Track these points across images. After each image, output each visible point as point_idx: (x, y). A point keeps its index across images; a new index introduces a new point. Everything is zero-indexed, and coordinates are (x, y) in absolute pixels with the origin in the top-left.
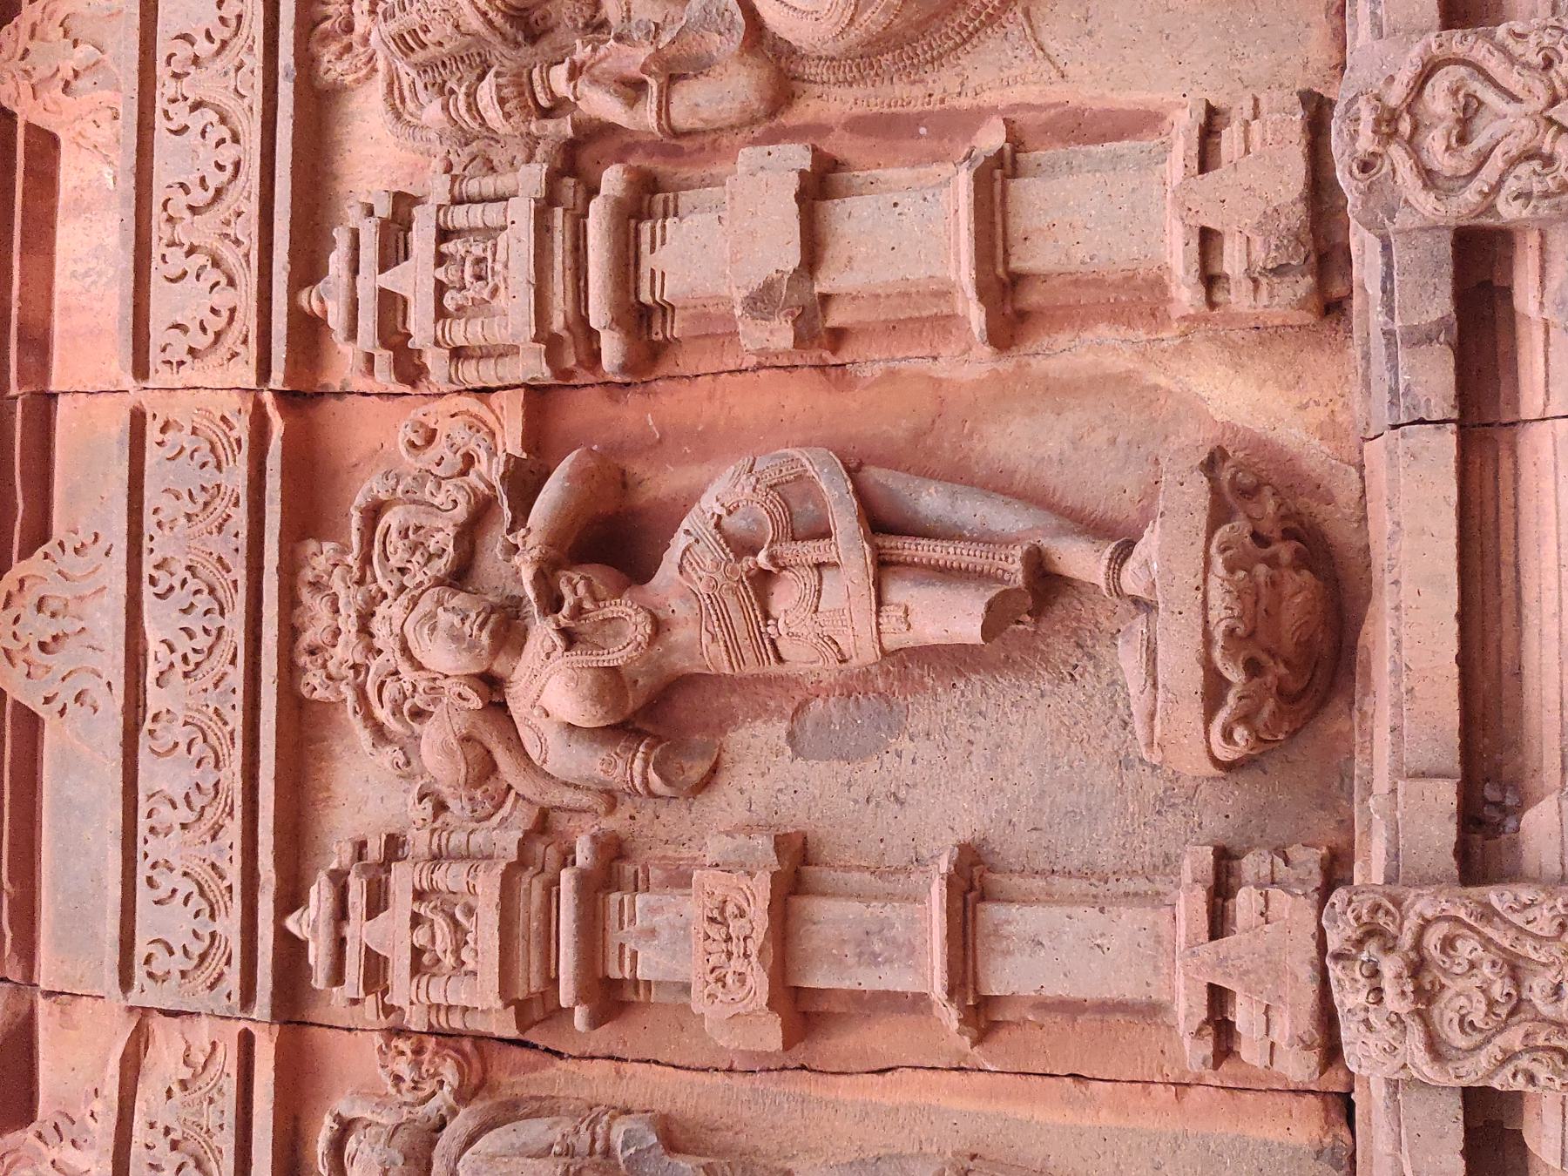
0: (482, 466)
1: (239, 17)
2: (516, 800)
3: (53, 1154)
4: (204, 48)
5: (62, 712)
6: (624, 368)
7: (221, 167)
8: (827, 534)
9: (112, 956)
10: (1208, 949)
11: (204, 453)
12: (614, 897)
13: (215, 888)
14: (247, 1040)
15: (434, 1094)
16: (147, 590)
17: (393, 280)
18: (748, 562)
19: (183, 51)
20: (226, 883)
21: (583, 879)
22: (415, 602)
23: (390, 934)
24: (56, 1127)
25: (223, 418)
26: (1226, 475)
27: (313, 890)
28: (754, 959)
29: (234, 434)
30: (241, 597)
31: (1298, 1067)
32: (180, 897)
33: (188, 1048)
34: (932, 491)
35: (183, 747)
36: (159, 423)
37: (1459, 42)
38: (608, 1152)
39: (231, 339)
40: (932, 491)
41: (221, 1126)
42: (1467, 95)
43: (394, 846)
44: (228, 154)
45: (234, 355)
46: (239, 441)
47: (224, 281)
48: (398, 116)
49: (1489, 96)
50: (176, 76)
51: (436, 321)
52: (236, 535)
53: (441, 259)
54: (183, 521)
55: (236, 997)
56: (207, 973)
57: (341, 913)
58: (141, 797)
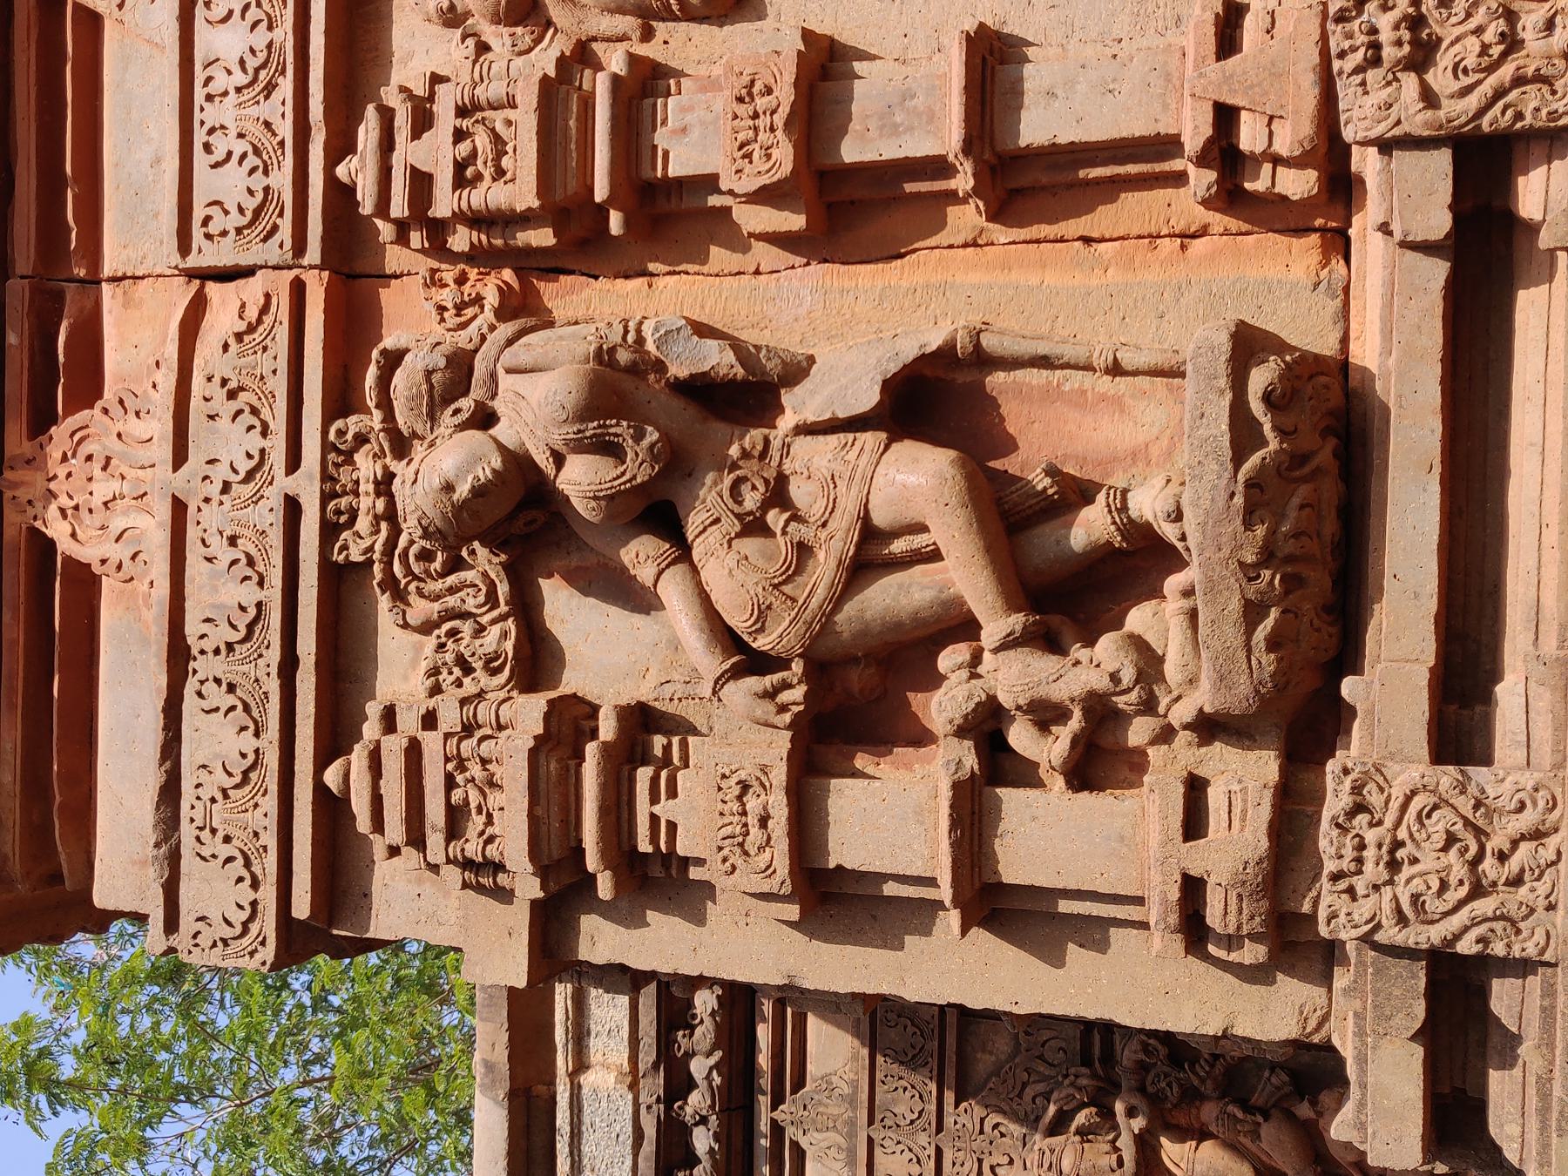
3: (119, 427)
9: (170, 221)
10: (1214, 69)
13: (268, 143)
15: (475, 316)
20: (279, 138)
23: (434, 152)
24: (121, 402)
28: (779, 133)
33: (243, 306)
35: (237, 13)
38: (640, 340)
41: (274, 372)
55: (288, 244)
56: (260, 228)
57: (387, 144)
58: (198, 67)
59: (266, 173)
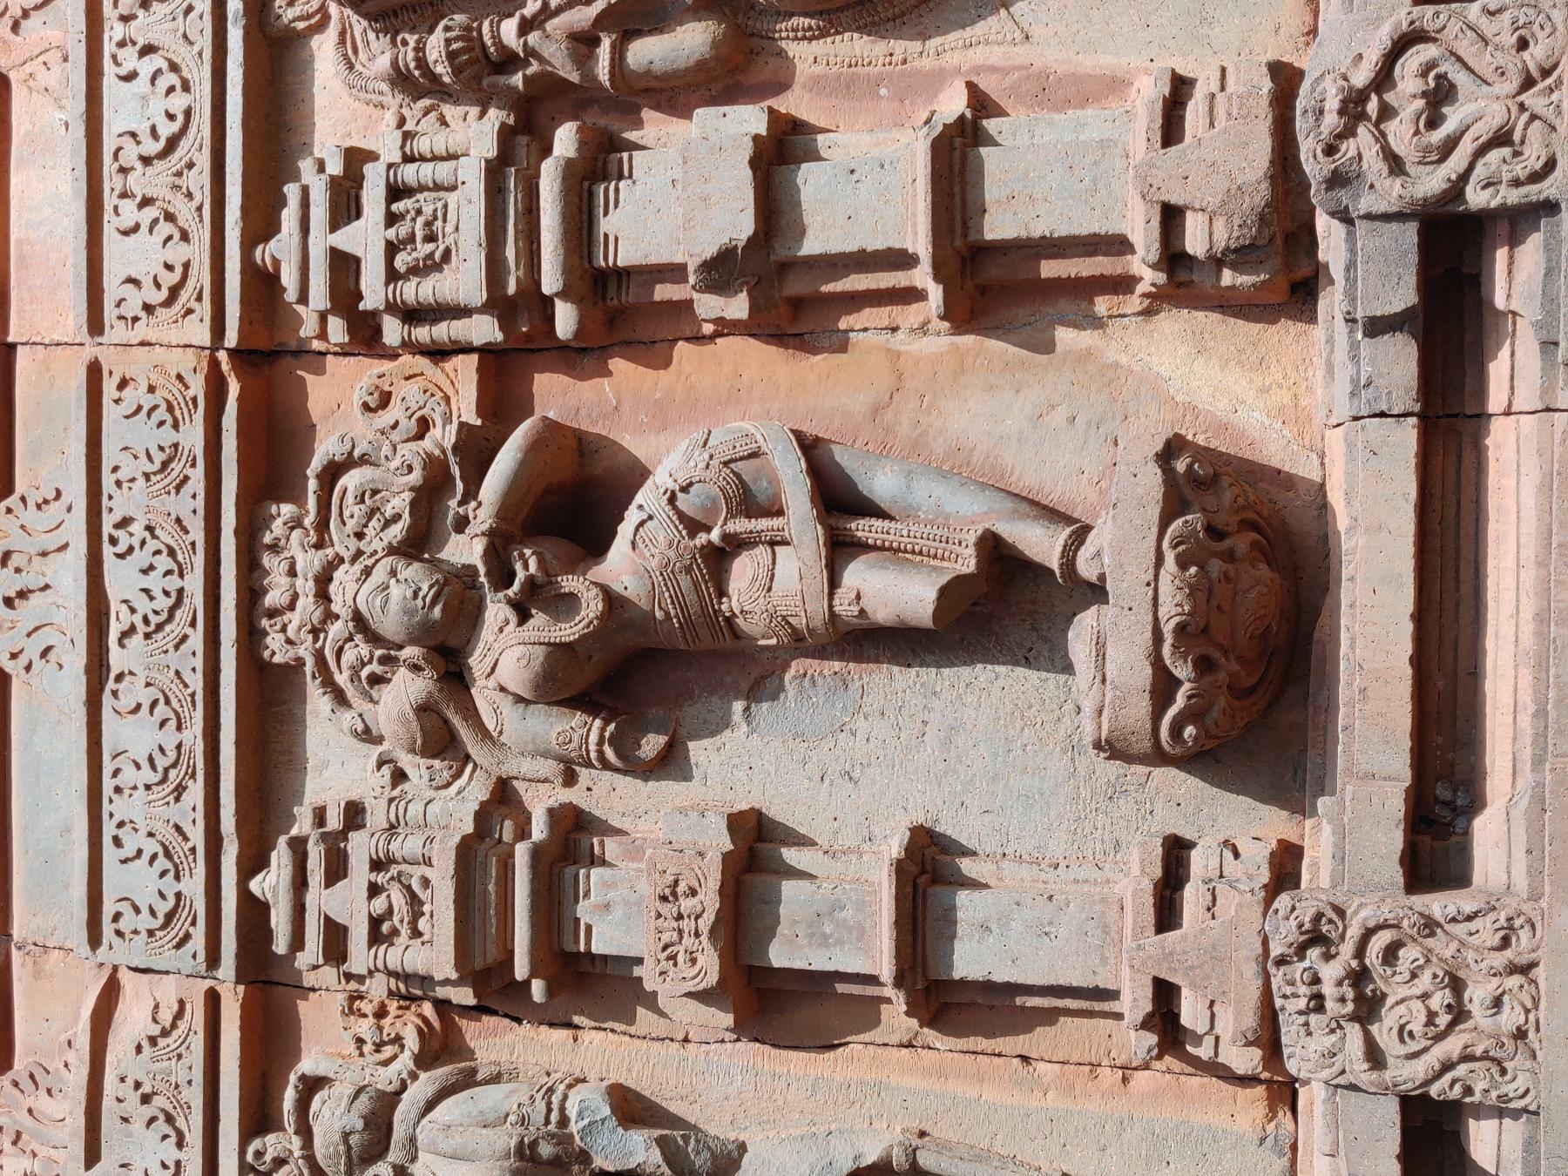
0: (435, 433)
2: (474, 771)
3: (30, 1102)
5: (28, 668)
6: (578, 334)
7: (171, 117)
8: (780, 513)
11: (162, 413)
12: (570, 870)
14: (213, 999)
15: (395, 1057)
17: (349, 239)
18: (702, 538)
20: (190, 845)
21: (537, 853)
22: (367, 572)
23: (347, 903)
24: (32, 1076)
25: (179, 377)
26: (1181, 466)
27: (274, 855)
28: (704, 938)
29: (191, 393)
30: (199, 559)
31: (1245, 1060)
32: (146, 857)
33: (157, 1006)
34: (888, 470)
35: (145, 709)
36: (116, 380)
39: (185, 296)
40: (888, 470)
41: (190, 1082)
43: (354, 814)
44: (178, 102)
45: (190, 311)
46: (194, 400)
47: (177, 236)
48: (351, 67)
50: (125, 19)
51: (387, 284)
52: (194, 497)
53: (392, 219)
54: (141, 481)
55: (201, 956)
58: (106, 758)
59: (177, 877)
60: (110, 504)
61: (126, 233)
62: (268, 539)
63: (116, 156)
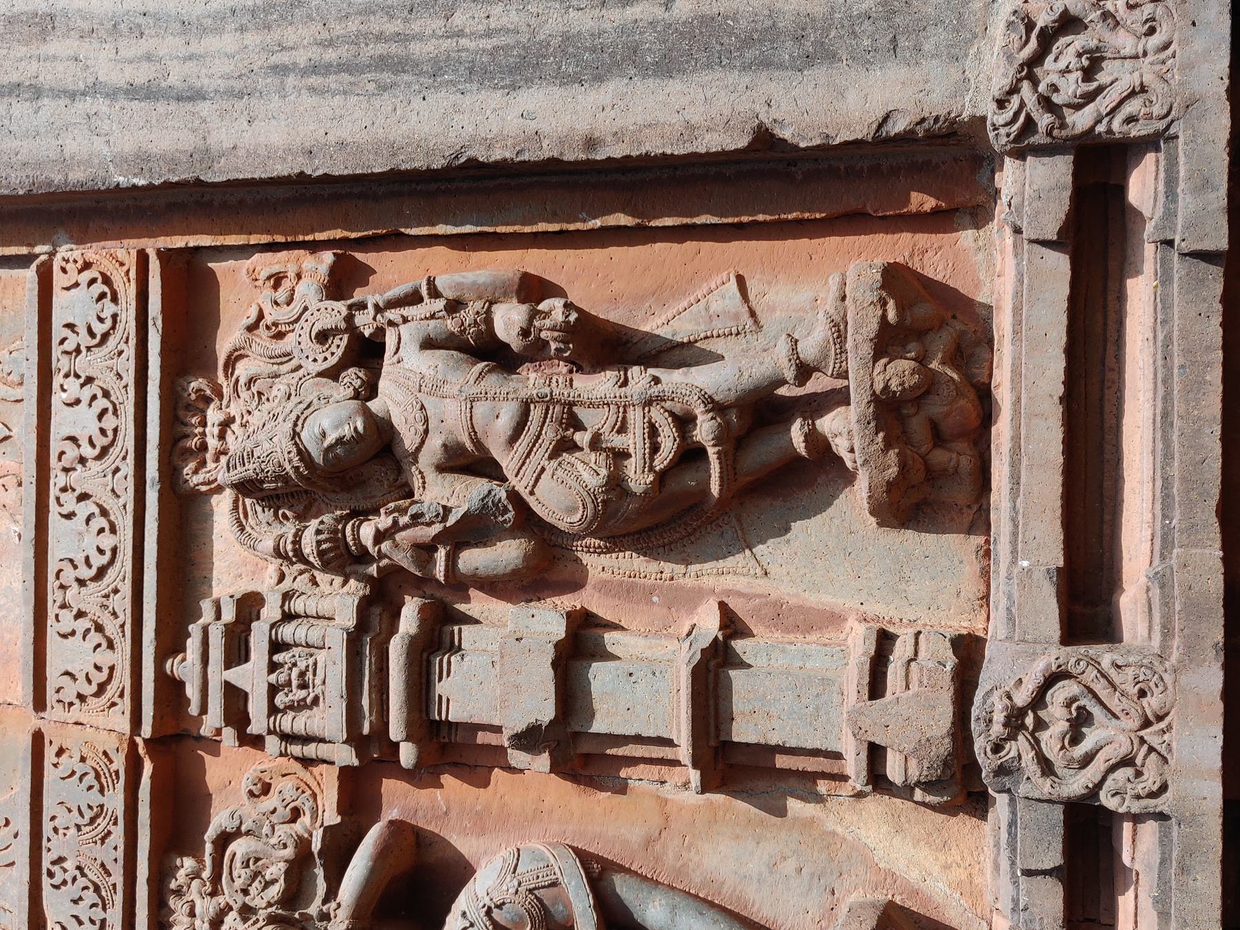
1: (115, 430)
4: (88, 452)
7: (101, 552)
11: (90, 779)
16: (46, 881)
17: (237, 676)
19: (72, 452)
25: (105, 753)
29: (113, 767)
30: (119, 898)
36: (55, 748)
37: (1071, 655)
39: (111, 690)
42: (1079, 708)
44: (107, 541)
45: (114, 704)
46: (117, 772)
47: (104, 645)
48: (242, 529)
49: (1096, 710)
50: (66, 470)
51: (269, 716)
52: (115, 848)
53: (273, 667)
54: (73, 831)
60: (49, 845)
61: (64, 636)
62: (173, 885)
63: (58, 577)
